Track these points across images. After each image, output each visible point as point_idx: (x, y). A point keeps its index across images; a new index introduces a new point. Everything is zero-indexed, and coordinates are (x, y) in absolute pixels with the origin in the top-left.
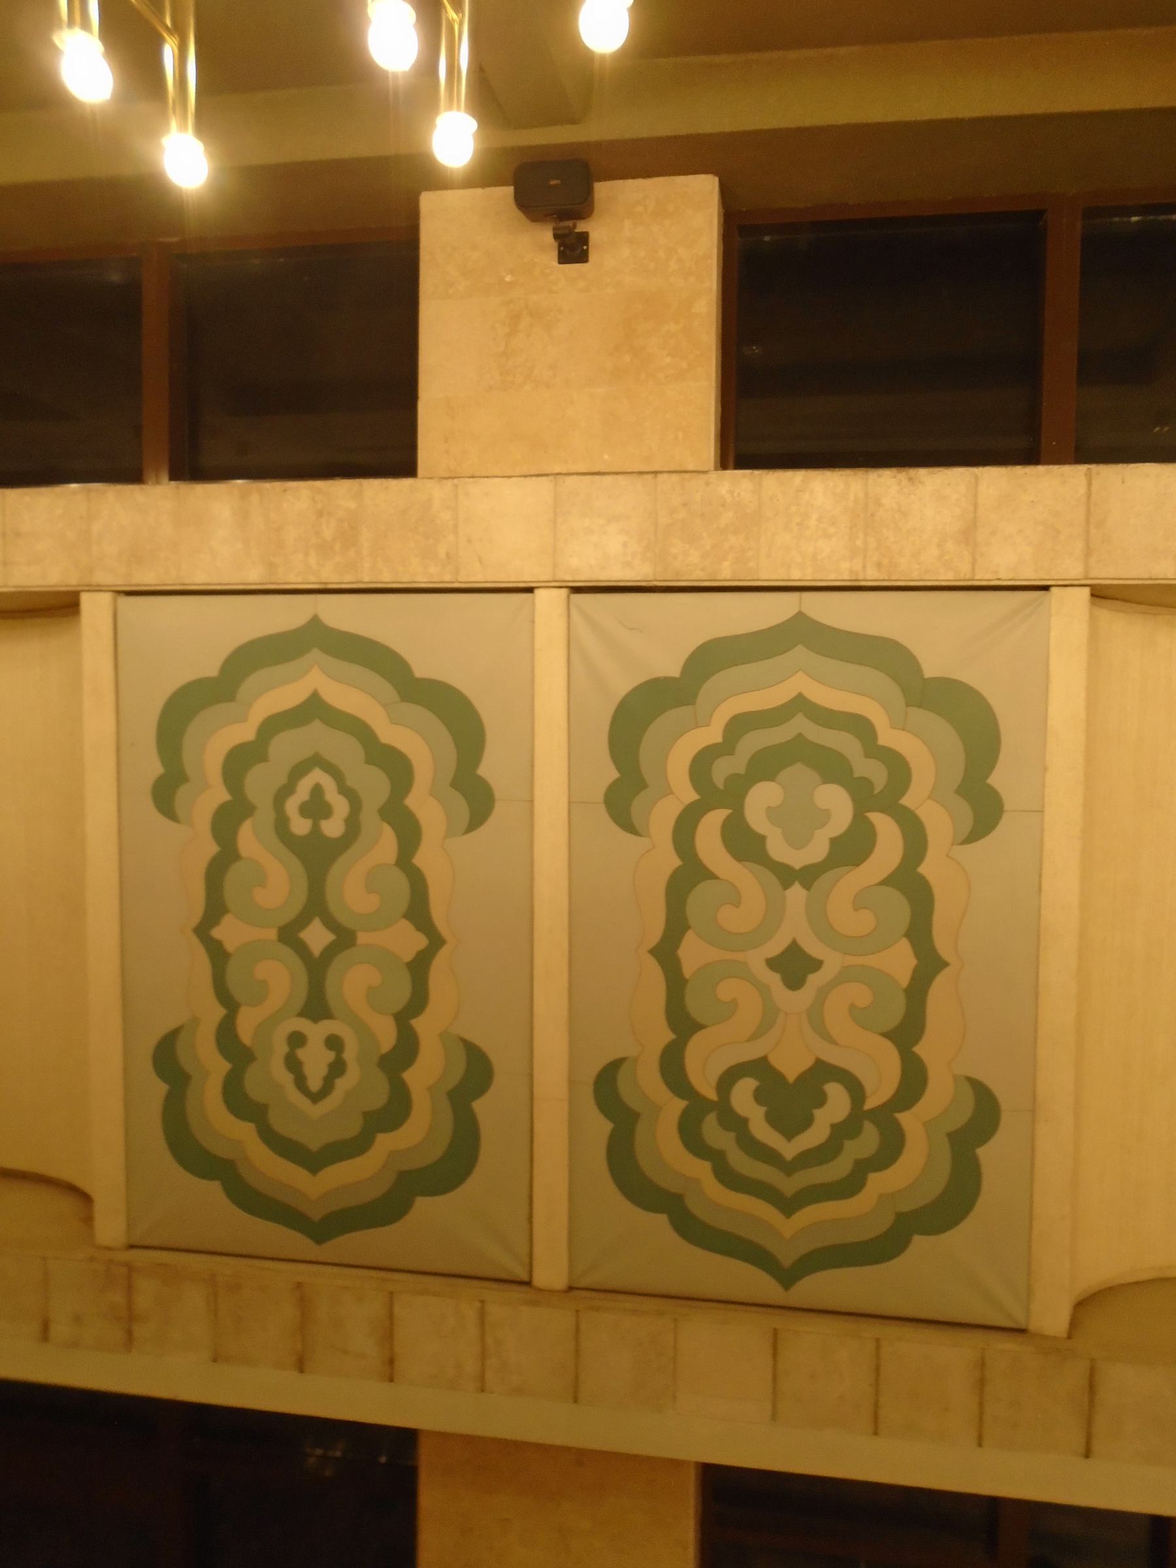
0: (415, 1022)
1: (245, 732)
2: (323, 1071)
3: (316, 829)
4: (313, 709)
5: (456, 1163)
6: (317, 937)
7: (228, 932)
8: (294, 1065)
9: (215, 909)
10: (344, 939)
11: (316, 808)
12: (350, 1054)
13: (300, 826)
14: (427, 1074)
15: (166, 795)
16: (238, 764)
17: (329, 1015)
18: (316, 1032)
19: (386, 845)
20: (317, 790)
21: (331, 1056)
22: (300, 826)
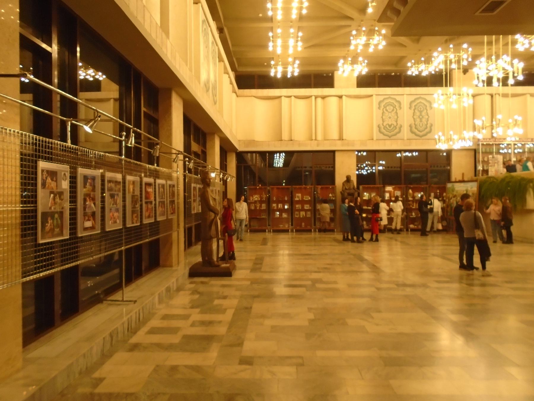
4: (420, 102)
5: (430, 131)
6: (421, 117)
7: (415, 117)
9: (414, 115)
10: (423, 117)
11: (421, 109)
14: (429, 125)
15: (410, 108)
16: (415, 106)
19: (425, 111)
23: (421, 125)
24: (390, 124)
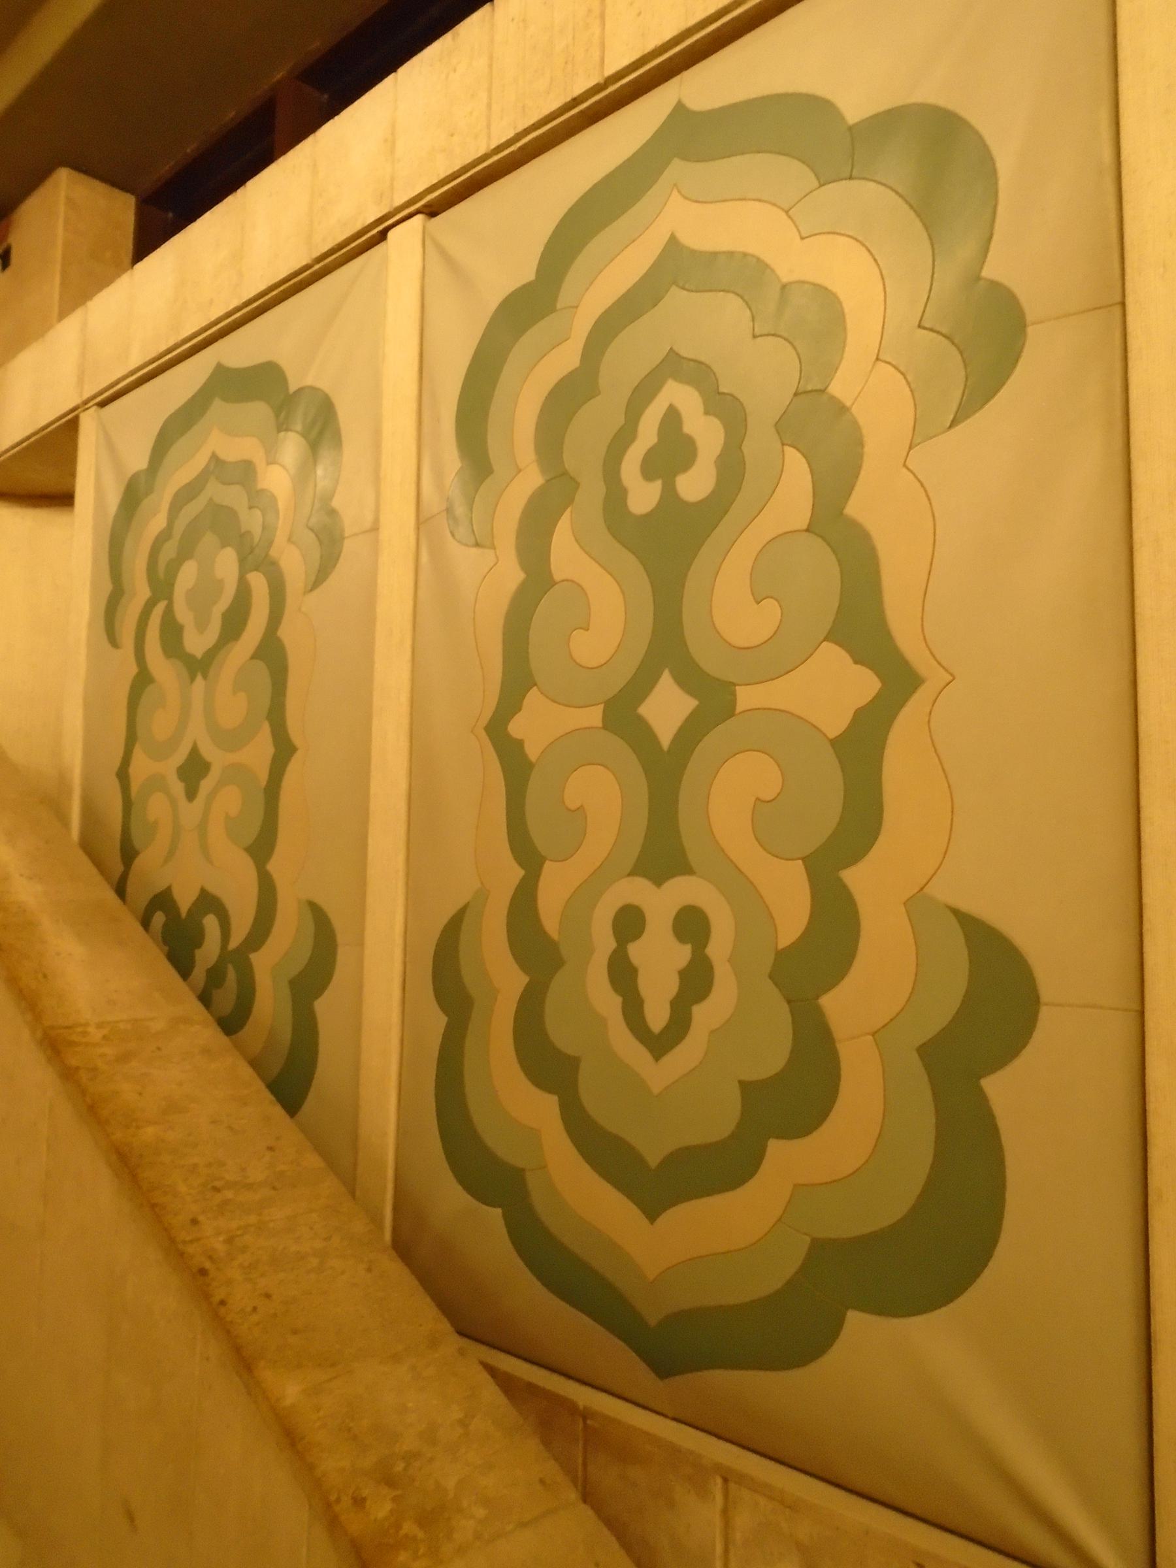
0: (853, 877)
1: (566, 358)
2: (672, 986)
3: (669, 490)
6: (667, 708)
8: (623, 975)
9: (517, 682)
10: (714, 702)
11: (673, 453)
12: (719, 948)
13: (643, 497)
17: (684, 868)
18: (660, 902)
20: (672, 417)
21: (683, 954)
22: (643, 497)
23: (660, 961)
24: (185, 900)
